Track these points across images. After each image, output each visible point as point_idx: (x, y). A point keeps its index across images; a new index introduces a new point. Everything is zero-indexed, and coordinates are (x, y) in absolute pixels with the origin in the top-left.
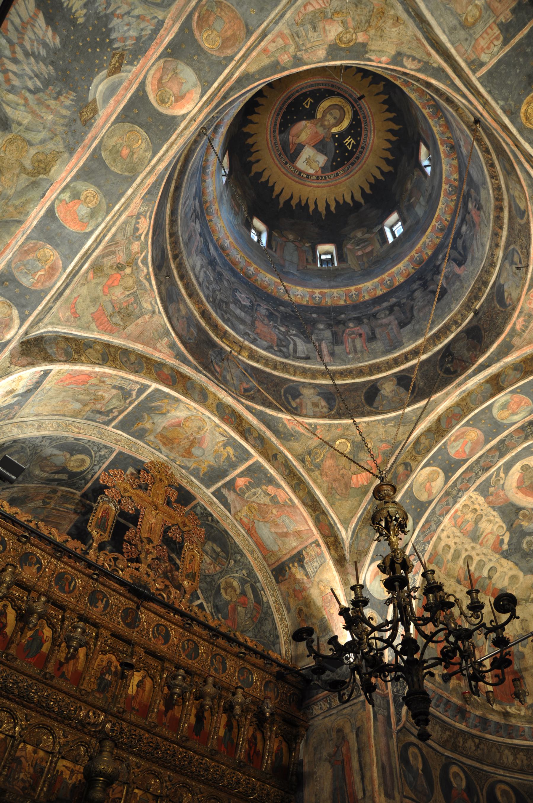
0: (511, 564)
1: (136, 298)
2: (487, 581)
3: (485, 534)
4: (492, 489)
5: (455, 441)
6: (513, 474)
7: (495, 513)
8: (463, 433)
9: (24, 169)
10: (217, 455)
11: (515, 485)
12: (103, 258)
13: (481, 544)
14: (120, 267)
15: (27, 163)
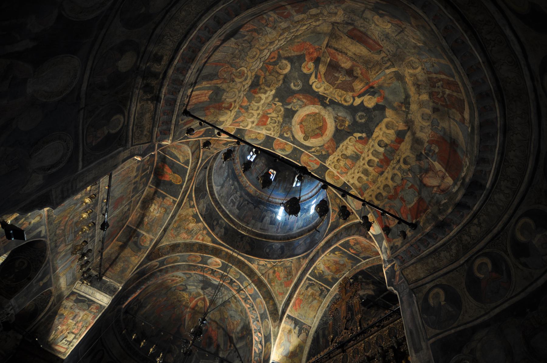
0: (376, 130)
1: (286, 268)
2: (388, 148)
3: (355, 150)
4: (324, 153)
5: (310, 166)
6: (312, 143)
7: (341, 146)
8: (305, 163)
9: (236, 302)
10: (343, 257)
11: (320, 139)
12: (269, 278)
13: (362, 153)
14: (274, 272)
15: (235, 301)
